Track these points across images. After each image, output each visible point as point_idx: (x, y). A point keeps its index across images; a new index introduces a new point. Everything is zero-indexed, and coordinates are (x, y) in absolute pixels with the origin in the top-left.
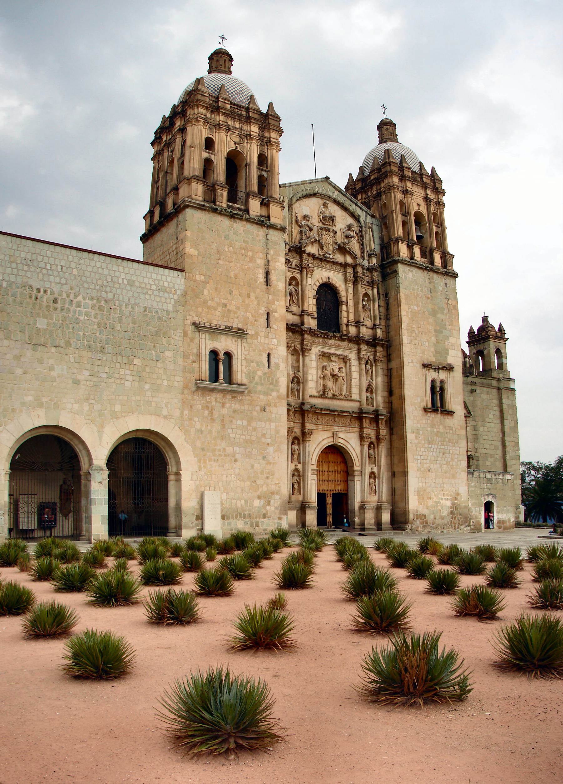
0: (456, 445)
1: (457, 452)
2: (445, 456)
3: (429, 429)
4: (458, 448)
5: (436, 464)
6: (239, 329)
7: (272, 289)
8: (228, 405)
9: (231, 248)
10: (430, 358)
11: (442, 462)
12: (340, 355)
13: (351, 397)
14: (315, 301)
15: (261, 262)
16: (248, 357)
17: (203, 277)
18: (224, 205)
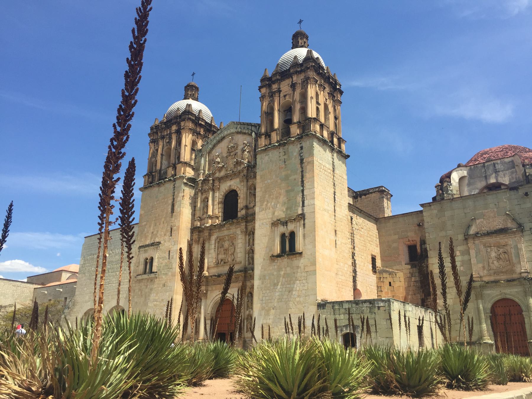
0: (304, 282)
1: (306, 288)
2: (291, 293)
3: (275, 273)
4: (307, 284)
5: (281, 302)
6: (157, 242)
7: (174, 214)
8: (149, 286)
9: (158, 202)
10: (280, 214)
11: (287, 300)
12: (229, 235)
13: (235, 261)
14: (220, 206)
15: (170, 202)
16: (159, 256)
17: (145, 223)
18: (156, 181)
